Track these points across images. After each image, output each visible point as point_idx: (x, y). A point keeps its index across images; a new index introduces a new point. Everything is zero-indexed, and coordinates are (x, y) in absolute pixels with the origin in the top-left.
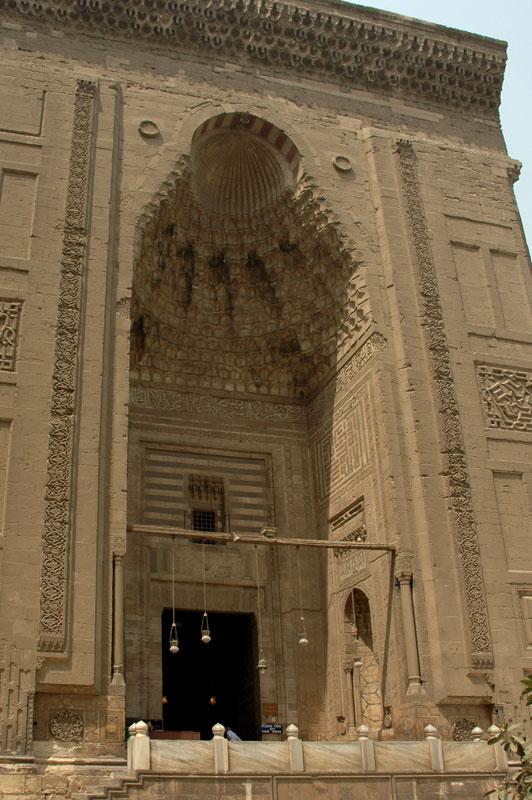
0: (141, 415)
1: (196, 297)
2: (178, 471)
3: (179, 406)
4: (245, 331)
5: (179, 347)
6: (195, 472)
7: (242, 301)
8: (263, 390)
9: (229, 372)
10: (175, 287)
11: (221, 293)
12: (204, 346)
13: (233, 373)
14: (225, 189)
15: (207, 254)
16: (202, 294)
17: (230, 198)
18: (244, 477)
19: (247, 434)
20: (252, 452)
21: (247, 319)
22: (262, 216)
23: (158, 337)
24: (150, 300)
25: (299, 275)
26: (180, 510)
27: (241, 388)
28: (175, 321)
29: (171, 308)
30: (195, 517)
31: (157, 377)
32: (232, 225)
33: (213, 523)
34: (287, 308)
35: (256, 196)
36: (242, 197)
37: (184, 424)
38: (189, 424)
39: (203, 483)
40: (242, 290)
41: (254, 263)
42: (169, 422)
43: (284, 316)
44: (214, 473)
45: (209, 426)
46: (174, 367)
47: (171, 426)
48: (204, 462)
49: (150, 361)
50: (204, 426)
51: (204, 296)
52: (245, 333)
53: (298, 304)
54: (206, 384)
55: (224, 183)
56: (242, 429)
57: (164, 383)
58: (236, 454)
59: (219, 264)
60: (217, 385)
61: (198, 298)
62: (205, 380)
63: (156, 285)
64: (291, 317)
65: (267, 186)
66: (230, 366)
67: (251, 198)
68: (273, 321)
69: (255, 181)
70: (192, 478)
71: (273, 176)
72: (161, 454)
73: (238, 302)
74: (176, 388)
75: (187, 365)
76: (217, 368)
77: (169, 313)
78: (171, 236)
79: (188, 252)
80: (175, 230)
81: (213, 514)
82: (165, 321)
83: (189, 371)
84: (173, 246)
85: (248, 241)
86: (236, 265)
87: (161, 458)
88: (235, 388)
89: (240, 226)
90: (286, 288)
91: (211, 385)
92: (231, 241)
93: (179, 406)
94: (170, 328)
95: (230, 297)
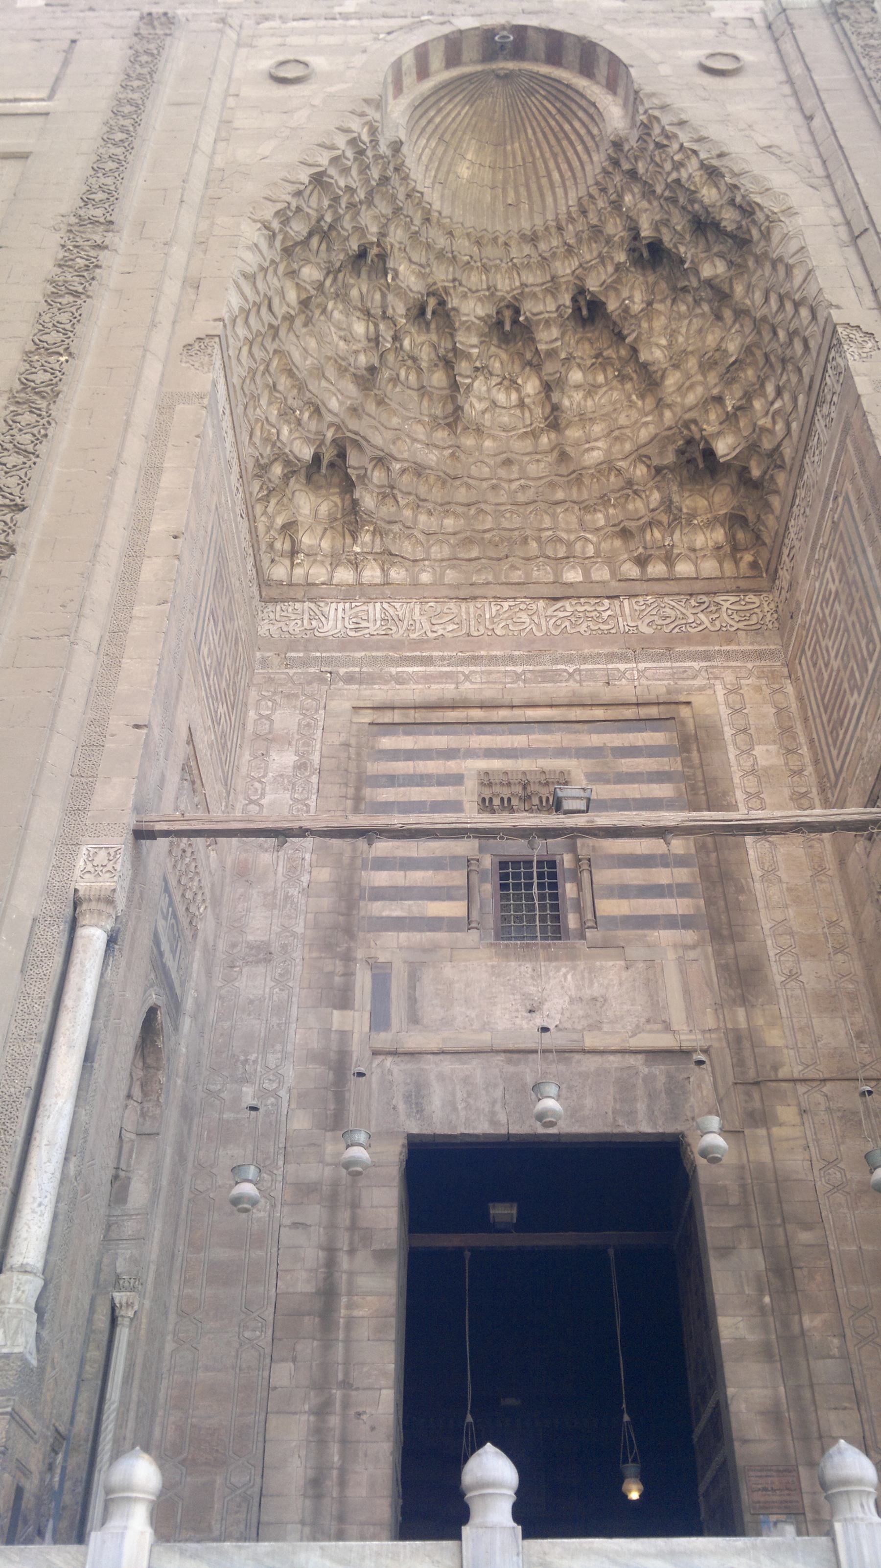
0: (358, 655)
1: (474, 407)
2: (452, 766)
3: (451, 627)
4: (595, 453)
5: (446, 507)
6: (496, 764)
7: (578, 396)
8: (657, 569)
9: (570, 545)
10: (422, 390)
11: (531, 386)
12: (503, 499)
13: (578, 546)
14: (504, 190)
15: (480, 312)
16: (484, 397)
17: (516, 205)
18: (626, 764)
19: (622, 666)
20: (638, 705)
21: (598, 429)
22: (584, 212)
23: (388, 493)
24: (354, 410)
25: (683, 308)
26: (454, 858)
27: (601, 574)
28: (432, 457)
29: (420, 431)
30: (504, 877)
31: (397, 574)
32: (527, 249)
33: (554, 886)
34: (672, 380)
35: (568, 183)
36: (542, 195)
37: (463, 662)
38: (475, 660)
39: (519, 790)
40: (576, 376)
41: (588, 312)
42: (427, 661)
43: (669, 400)
44: (545, 763)
45: (528, 660)
46: (436, 551)
47: (431, 669)
48: (518, 741)
49: (378, 541)
50: (512, 660)
51: (494, 404)
52: (596, 456)
53: (692, 363)
54: (517, 576)
55: (500, 177)
56: (611, 657)
57: (416, 584)
58: (599, 713)
59: (510, 327)
60: (542, 573)
61: (479, 406)
62: (513, 567)
63: (366, 380)
64: (683, 396)
65: (585, 157)
66: (569, 531)
67: (560, 192)
68: (649, 418)
69: (561, 159)
70: (486, 780)
71: (589, 132)
72: (406, 733)
73: (571, 401)
74: (445, 592)
75: (468, 541)
76: (538, 540)
77: (415, 440)
78: (386, 275)
79: (433, 311)
80: (391, 264)
81: (552, 864)
82: (406, 455)
83: (474, 554)
84: (390, 297)
85: (565, 269)
86: (547, 322)
87: (406, 742)
88: (586, 573)
89: (543, 246)
90: (663, 342)
91: (528, 574)
92: (529, 278)
93: (451, 627)
94: (419, 470)
95: (547, 387)
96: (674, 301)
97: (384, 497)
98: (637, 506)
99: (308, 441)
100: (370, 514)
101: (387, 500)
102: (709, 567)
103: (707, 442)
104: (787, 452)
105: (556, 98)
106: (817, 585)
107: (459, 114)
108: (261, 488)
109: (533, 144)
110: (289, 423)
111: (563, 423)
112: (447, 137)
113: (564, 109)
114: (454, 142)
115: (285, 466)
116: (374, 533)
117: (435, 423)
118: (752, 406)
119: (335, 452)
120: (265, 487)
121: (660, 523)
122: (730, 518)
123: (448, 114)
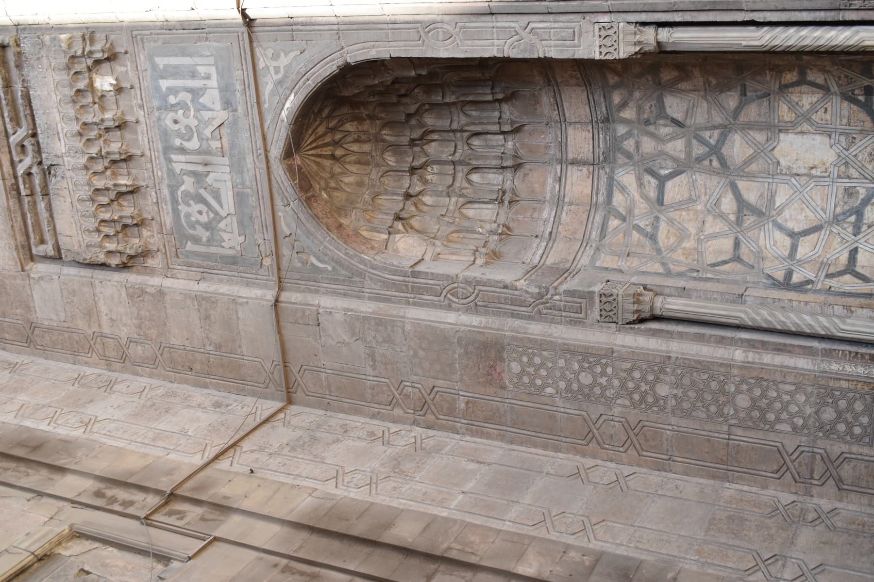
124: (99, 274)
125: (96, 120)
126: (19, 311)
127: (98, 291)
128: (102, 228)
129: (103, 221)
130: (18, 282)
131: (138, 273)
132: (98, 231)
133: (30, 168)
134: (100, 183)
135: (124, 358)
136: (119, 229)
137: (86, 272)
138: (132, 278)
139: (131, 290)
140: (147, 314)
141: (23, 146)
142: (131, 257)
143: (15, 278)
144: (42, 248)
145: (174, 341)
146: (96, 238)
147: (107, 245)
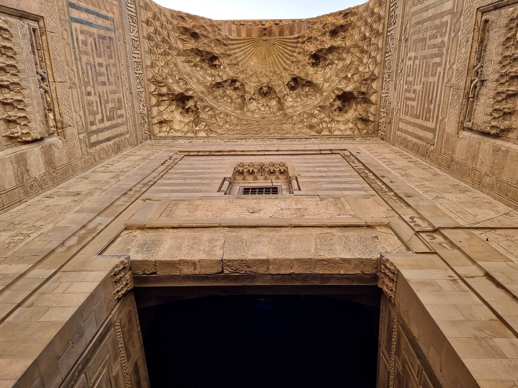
96: (325, 69)
97: (211, 118)
98: (314, 120)
99: (181, 89)
100: (204, 119)
101: (212, 119)
102: (349, 132)
103: (342, 90)
104: (376, 72)
105: (282, 44)
106: (402, 82)
107: (251, 49)
108: (155, 90)
109: (275, 58)
110: (173, 80)
111: (285, 108)
112: (247, 54)
113: (285, 46)
114: (249, 56)
115: (168, 91)
116: (205, 126)
117: (236, 109)
118: (359, 71)
119: (193, 104)
120: (157, 91)
121: (325, 122)
122: (355, 121)
123: (247, 48)
124: (486, 139)
125: (510, 54)
126: (450, 153)
127: (481, 146)
128: (493, 114)
129: (495, 110)
130: (454, 139)
131: (503, 140)
132: (491, 115)
133: (477, 83)
134: (500, 89)
135: (480, 182)
136: (501, 115)
137: (480, 137)
138: (499, 142)
139: (495, 148)
140: (498, 161)
141: (478, 73)
142: (502, 131)
143: (453, 137)
144: (468, 123)
145: (505, 178)
146: (489, 118)
147: (493, 122)
